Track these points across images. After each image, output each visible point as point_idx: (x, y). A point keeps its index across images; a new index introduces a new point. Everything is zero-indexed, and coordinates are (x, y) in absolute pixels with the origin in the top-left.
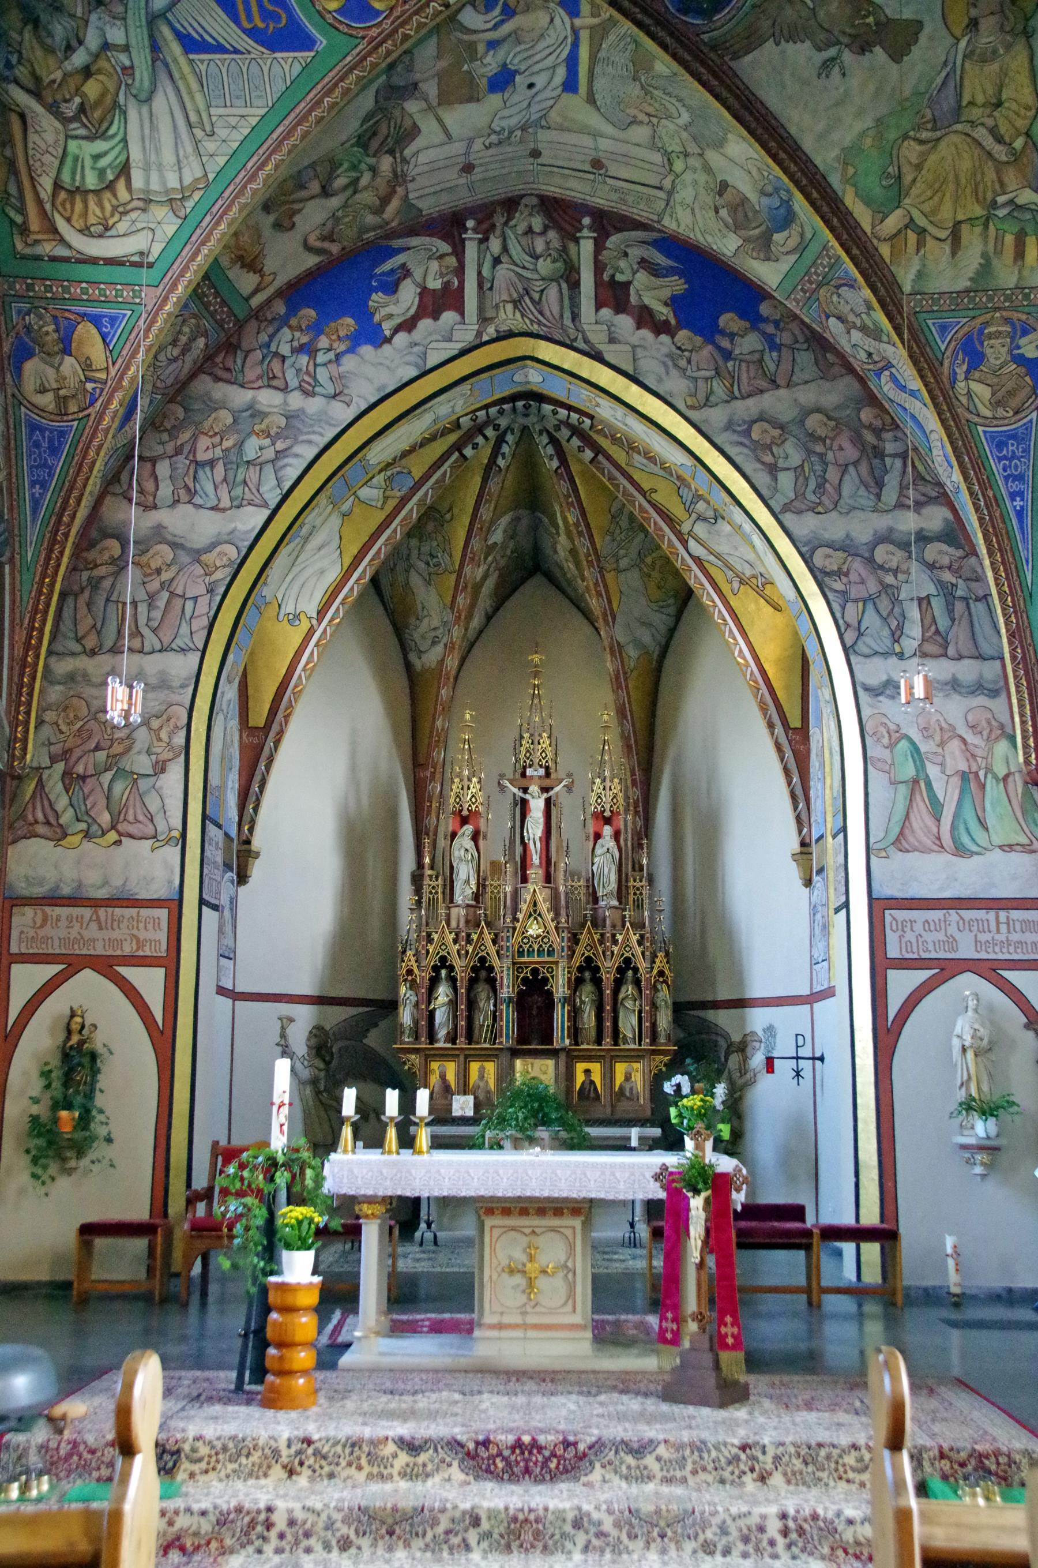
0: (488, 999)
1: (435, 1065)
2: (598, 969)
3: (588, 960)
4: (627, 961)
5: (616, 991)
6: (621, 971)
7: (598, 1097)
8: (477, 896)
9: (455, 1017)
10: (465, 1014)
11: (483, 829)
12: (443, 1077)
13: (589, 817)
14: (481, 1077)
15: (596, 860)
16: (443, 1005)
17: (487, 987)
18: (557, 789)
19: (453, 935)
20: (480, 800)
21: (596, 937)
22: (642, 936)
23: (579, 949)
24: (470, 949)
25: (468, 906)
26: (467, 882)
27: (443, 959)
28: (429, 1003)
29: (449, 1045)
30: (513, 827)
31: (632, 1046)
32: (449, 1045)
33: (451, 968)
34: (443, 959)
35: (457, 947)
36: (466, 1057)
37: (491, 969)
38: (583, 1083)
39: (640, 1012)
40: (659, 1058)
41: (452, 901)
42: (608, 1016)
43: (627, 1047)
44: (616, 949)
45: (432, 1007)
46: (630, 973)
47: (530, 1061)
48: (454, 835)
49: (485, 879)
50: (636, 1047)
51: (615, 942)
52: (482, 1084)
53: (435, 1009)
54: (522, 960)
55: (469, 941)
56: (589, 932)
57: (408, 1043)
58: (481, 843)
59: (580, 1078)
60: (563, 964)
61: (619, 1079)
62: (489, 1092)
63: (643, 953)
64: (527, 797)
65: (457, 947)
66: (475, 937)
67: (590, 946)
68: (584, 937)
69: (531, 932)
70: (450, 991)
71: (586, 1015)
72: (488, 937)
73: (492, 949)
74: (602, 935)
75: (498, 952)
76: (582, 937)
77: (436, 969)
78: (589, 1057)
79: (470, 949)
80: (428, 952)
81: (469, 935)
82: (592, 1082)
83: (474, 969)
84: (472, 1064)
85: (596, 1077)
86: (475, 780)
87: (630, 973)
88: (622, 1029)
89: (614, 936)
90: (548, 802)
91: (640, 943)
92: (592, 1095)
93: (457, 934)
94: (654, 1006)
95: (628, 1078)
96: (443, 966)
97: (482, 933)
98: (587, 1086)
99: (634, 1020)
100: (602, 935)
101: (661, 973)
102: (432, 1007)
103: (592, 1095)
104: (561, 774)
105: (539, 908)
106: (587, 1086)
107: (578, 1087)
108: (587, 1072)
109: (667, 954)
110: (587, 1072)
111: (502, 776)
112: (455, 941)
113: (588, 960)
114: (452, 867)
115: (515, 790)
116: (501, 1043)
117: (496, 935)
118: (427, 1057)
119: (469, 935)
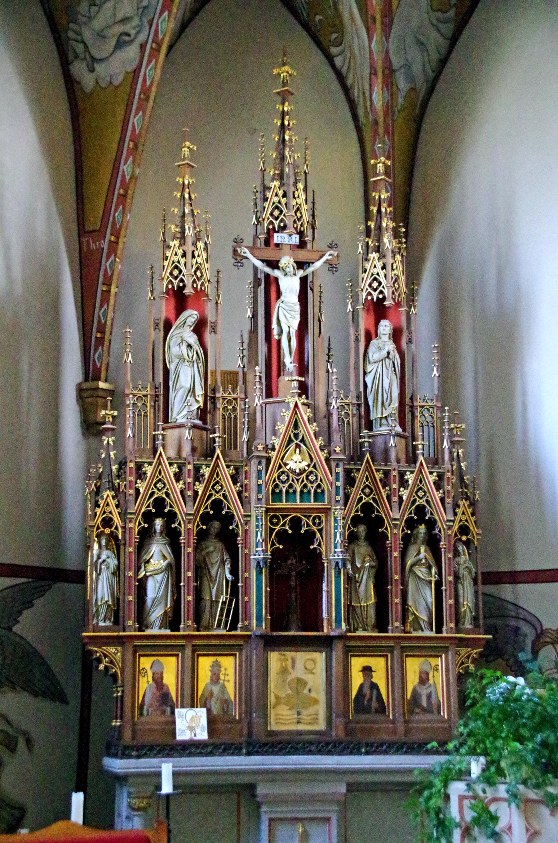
0: (223, 563)
1: (146, 663)
2: (380, 521)
3: (367, 508)
4: (420, 510)
5: (404, 554)
6: (411, 524)
7: (382, 709)
8: (203, 413)
9: (177, 589)
10: (193, 584)
11: (210, 317)
12: (158, 681)
13: (360, 307)
14: (215, 678)
15: (369, 368)
16: (157, 572)
17: (220, 545)
18: (318, 264)
19: (175, 468)
20: (207, 275)
21: (379, 476)
22: (440, 476)
23: (355, 493)
24: (200, 488)
25: (194, 426)
26: (192, 391)
27: (159, 503)
28: (139, 568)
29: (168, 632)
30: (255, 316)
31: (427, 633)
32: (168, 632)
33: (171, 517)
34: (159, 503)
35: (180, 486)
36: (195, 648)
37: (230, 518)
38: (362, 686)
39: (439, 584)
40: (464, 651)
41: (166, 420)
42: (394, 589)
43: (419, 634)
44: (405, 494)
45: (142, 574)
46: (422, 529)
47: (289, 654)
48: (168, 326)
49: (214, 390)
50: (433, 634)
51: (403, 483)
52: (216, 689)
53: (146, 577)
54: (278, 505)
55: (198, 477)
56: (368, 468)
57: (106, 629)
58: (209, 337)
59: (357, 680)
60: (338, 511)
61: (412, 681)
62: (226, 702)
63: (442, 500)
64: (276, 273)
65: (180, 486)
66: (206, 471)
67: (370, 489)
68: (360, 477)
69: (292, 465)
70: (167, 551)
71: (362, 588)
72: (226, 473)
73: (232, 490)
74: (387, 473)
75: (239, 493)
76: (359, 476)
77: (148, 517)
78: (363, 652)
79: (200, 488)
80: (137, 491)
81: (197, 469)
82: (374, 686)
83: (206, 518)
84: (201, 659)
85: (379, 678)
86: (201, 245)
87: (422, 529)
88: (412, 609)
89: (402, 474)
90: (304, 281)
91: (438, 485)
92: (374, 704)
93: (179, 467)
94: (457, 577)
95: (424, 679)
96: (160, 513)
97: (216, 465)
98: (367, 690)
99: (430, 596)
100: (387, 473)
101: (464, 530)
102: (142, 574)
103: (374, 704)
104: (321, 243)
105: (302, 432)
106: (367, 690)
107: (354, 693)
108: (367, 670)
109: (473, 504)
110: (367, 670)
111: (238, 242)
112: (178, 476)
113: (367, 508)
114: (166, 372)
115: (259, 264)
116: (246, 628)
117: (237, 469)
118: (136, 649)
119: (197, 469)
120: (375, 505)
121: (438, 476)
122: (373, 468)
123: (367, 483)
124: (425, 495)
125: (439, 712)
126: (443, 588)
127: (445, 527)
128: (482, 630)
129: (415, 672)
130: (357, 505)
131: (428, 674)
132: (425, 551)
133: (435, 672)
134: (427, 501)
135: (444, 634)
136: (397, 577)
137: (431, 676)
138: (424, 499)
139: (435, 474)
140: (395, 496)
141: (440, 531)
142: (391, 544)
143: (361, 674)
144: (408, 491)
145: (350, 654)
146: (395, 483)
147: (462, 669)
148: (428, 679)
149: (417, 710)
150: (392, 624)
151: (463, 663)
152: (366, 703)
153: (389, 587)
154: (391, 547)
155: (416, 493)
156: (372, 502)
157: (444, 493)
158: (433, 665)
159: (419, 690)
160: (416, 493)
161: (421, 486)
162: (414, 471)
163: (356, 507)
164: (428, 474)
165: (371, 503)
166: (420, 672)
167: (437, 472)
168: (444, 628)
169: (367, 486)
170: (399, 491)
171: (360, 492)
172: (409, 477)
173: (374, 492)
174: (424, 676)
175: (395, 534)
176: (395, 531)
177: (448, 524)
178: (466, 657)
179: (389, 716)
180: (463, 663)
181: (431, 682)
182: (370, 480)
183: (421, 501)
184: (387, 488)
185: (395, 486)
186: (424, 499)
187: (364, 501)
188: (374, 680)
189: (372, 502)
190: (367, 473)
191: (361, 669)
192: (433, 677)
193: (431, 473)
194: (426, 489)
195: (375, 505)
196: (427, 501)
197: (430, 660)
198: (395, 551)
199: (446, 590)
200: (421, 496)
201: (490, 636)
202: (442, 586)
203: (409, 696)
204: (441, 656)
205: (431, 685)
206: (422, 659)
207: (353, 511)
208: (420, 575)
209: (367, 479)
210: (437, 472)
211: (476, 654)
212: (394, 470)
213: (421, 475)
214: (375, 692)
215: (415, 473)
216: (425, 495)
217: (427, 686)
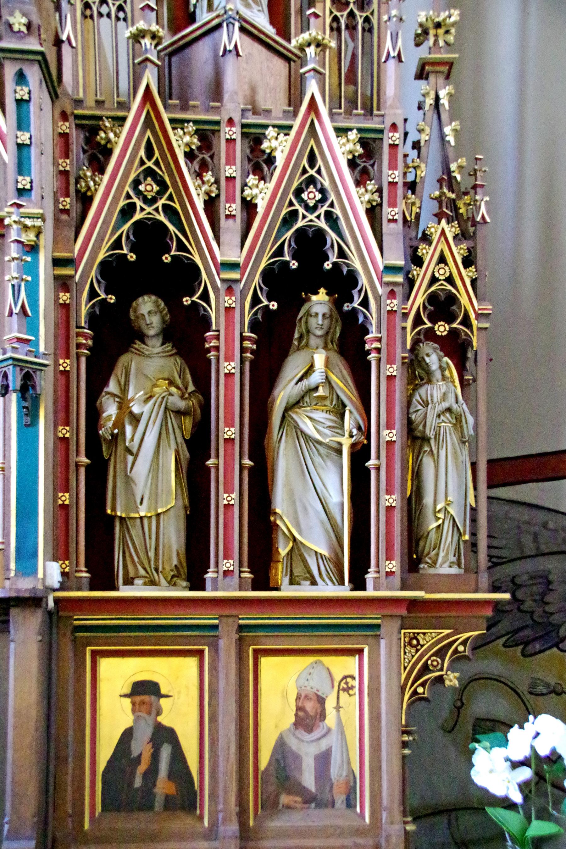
38: (128, 735)
120: (171, 227)
121: (363, 142)
122: (165, 116)
123: (150, 164)
124: (323, 200)
125: (350, 804)
126: (372, 463)
127: (380, 290)
128: (484, 579)
129: (285, 696)
130: (115, 229)
131: (321, 701)
132: (327, 364)
133: (343, 695)
134: (329, 216)
135: (370, 592)
136: (231, 432)
137: (330, 704)
138: (322, 211)
139: (353, 135)
140: (230, 199)
141: (365, 303)
142: (217, 338)
143: (127, 702)
144: (271, 185)
145: (89, 649)
146: (230, 161)
147: (423, 685)
148: (323, 716)
149: (285, 799)
150: (217, 565)
151: (425, 669)
152: (138, 782)
153: (211, 462)
154: (217, 348)
155: (298, 192)
156: (162, 217)
157: (380, 191)
158: (338, 677)
159: (293, 743)
160: (298, 192)
161: (312, 172)
162: (290, 127)
163: (112, 234)
164: (332, 134)
165: (162, 223)
166: (298, 698)
167: (360, 130)
168: (370, 576)
169: (149, 172)
170: (244, 185)
171: (127, 188)
172: (274, 143)
173: (171, 190)
174: (310, 706)
175: (229, 309)
176: (229, 301)
177: (388, 278)
178: (436, 654)
179: (201, 818)
180: (425, 669)
181: (331, 720)
182: (157, 154)
183: (310, 217)
184: (208, 176)
185: (229, 171)
186: (322, 211)
187: (138, 216)
188: (165, 720)
189: (162, 217)
190: (149, 133)
191: (127, 690)
192: (338, 708)
193: (341, 131)
194: (327, 184)
195: (171, 227)
196: (329, 216)
197: (328, 661)
198: (228, 358)
199: (378, 469)
200: (311, 203)
201: (507, 596)
202: (369, 459)
203: (264, 761)
204: (360, 652)
205: (329, 730)
206: (310, 660)
207: (105, 246)
208: (309, 428)
209: (150, 153)
210: (360, 130)
211: (464, 643)
212: (231, 122)
213: (312, 142)
214: (166, 752)
215: (293, 133)
216: (323, 200)
217: (316, 734)
